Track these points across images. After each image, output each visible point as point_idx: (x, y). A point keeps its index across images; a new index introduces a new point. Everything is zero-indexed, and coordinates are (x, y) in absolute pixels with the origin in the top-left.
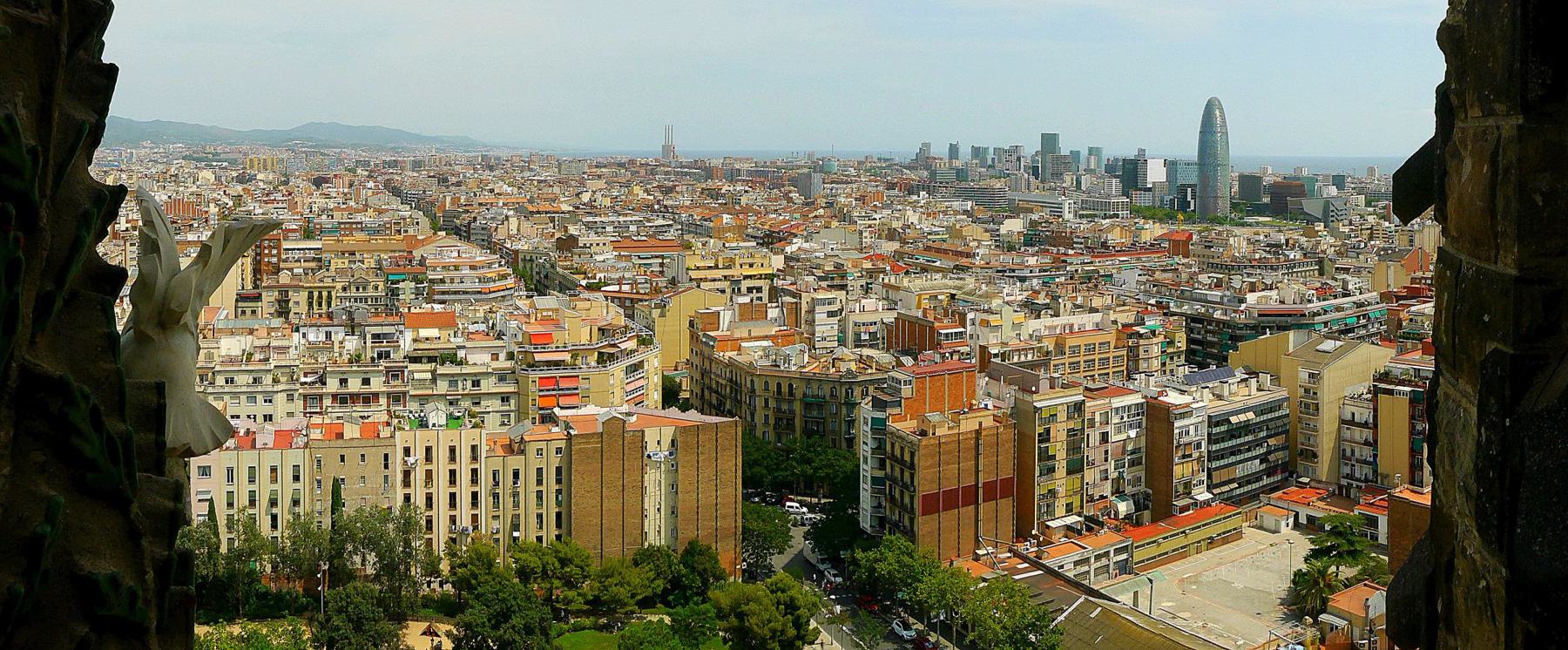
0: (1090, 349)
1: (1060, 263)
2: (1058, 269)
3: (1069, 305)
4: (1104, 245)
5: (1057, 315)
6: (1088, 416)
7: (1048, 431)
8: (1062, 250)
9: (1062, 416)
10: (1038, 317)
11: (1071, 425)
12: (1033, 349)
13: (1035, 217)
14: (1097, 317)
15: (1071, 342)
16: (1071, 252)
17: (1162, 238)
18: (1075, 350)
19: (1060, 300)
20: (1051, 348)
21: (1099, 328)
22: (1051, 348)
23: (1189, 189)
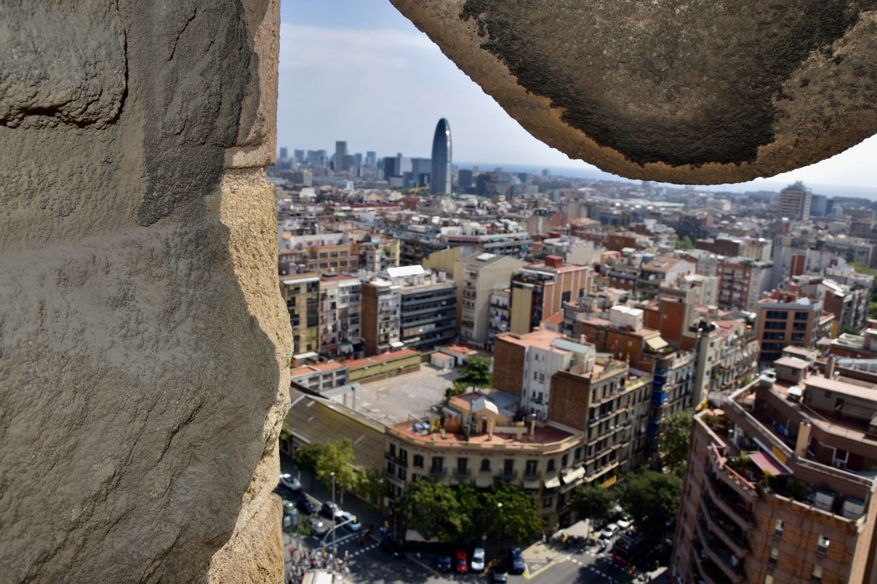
0: (334, 255)
1: (329, 210)
2: (328, 214)
3: (323, 228)
4: (361, 201)
5: (314, 233)
6: (322, 292)
7: (294, 299)
8: (332, 202)
9: (303, 290)
10: (301, 234)
11: (310, 296)
12: (295, 254)
13: (324, 188)
14: (339, 236)
15: (322, 251)
16: (337, 204)
17: (400, 200)
18: (324, 255)
19: (316, 225)
20: (308, 254)
21: (341, 242)
22: (308, 254)
23: (426, 178)
